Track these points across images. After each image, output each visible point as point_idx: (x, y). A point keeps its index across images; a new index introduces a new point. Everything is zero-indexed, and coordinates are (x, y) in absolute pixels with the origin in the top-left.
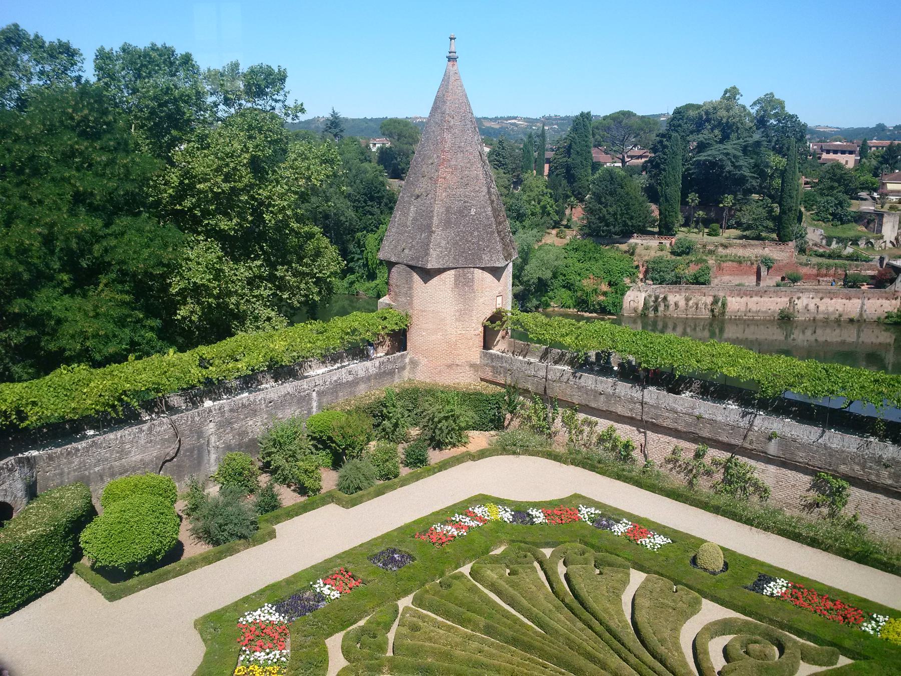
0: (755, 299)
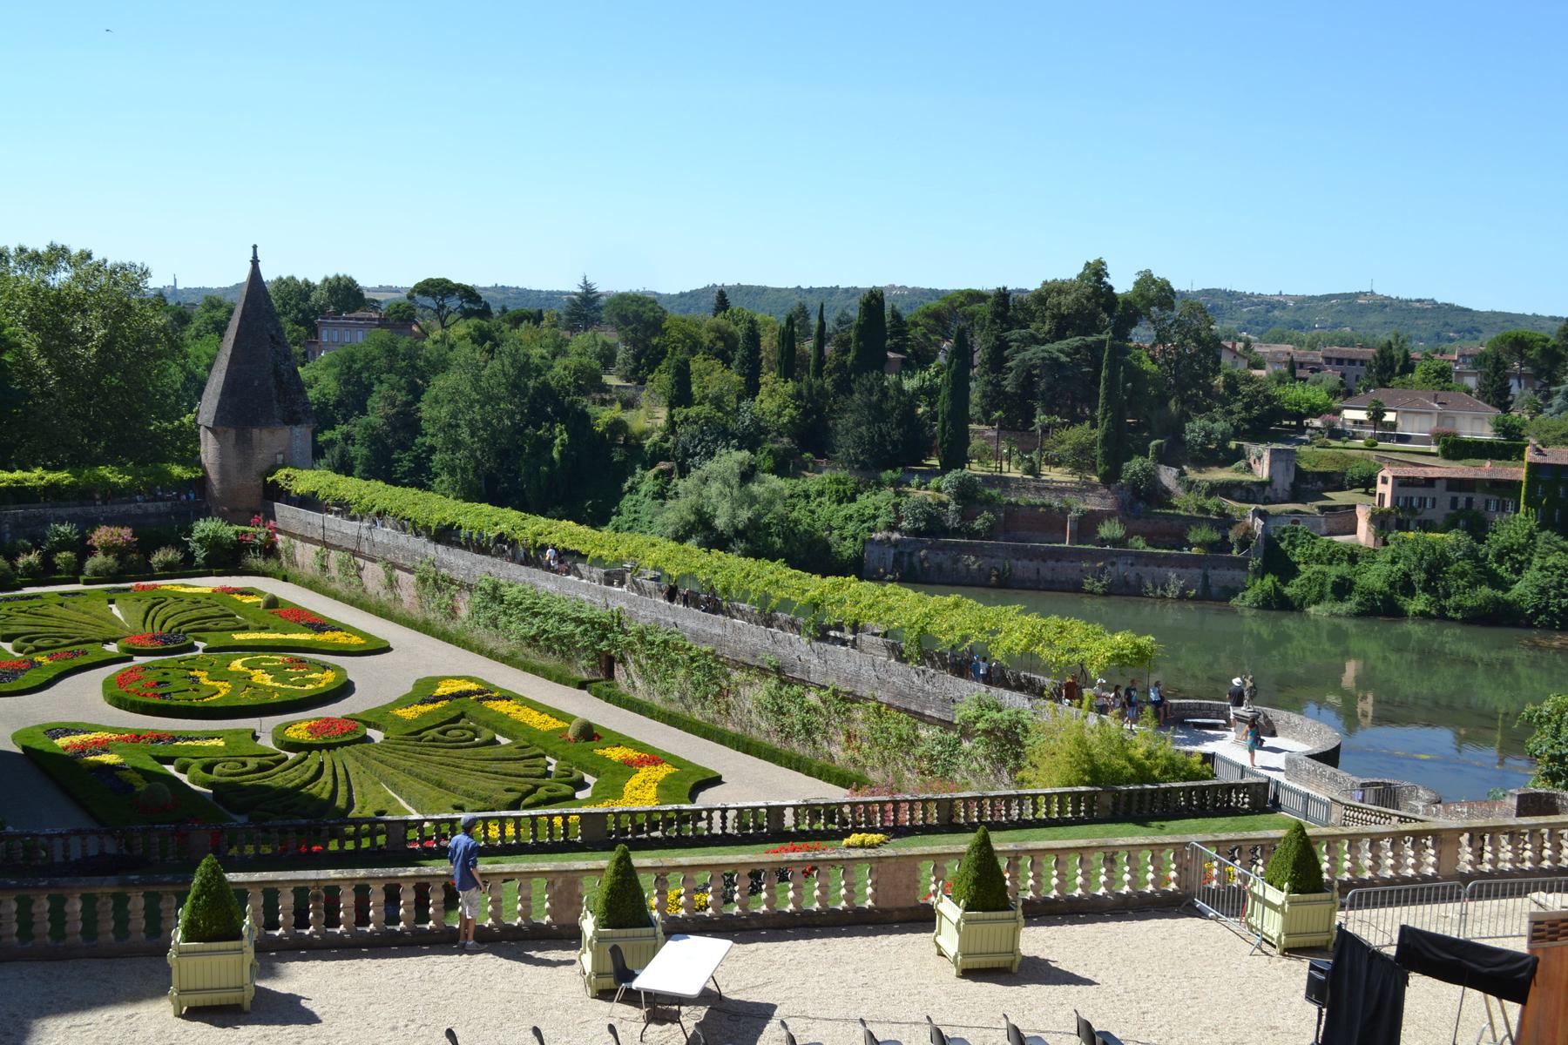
0: (1051, 563)
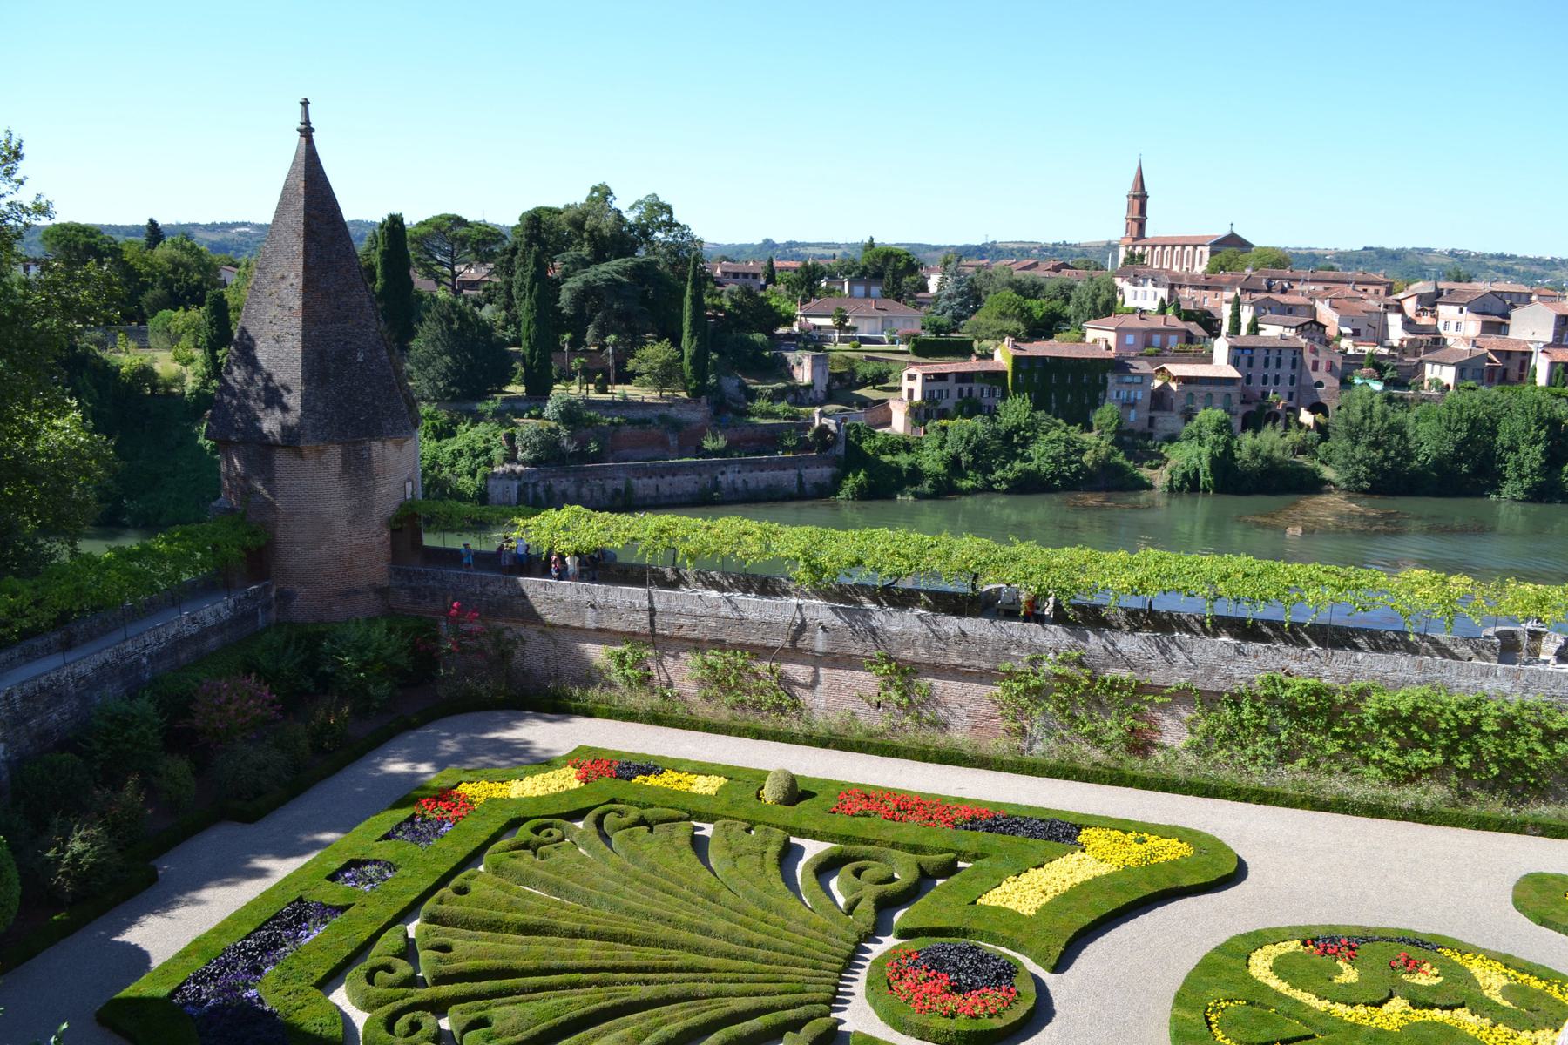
0: (668, 478)
